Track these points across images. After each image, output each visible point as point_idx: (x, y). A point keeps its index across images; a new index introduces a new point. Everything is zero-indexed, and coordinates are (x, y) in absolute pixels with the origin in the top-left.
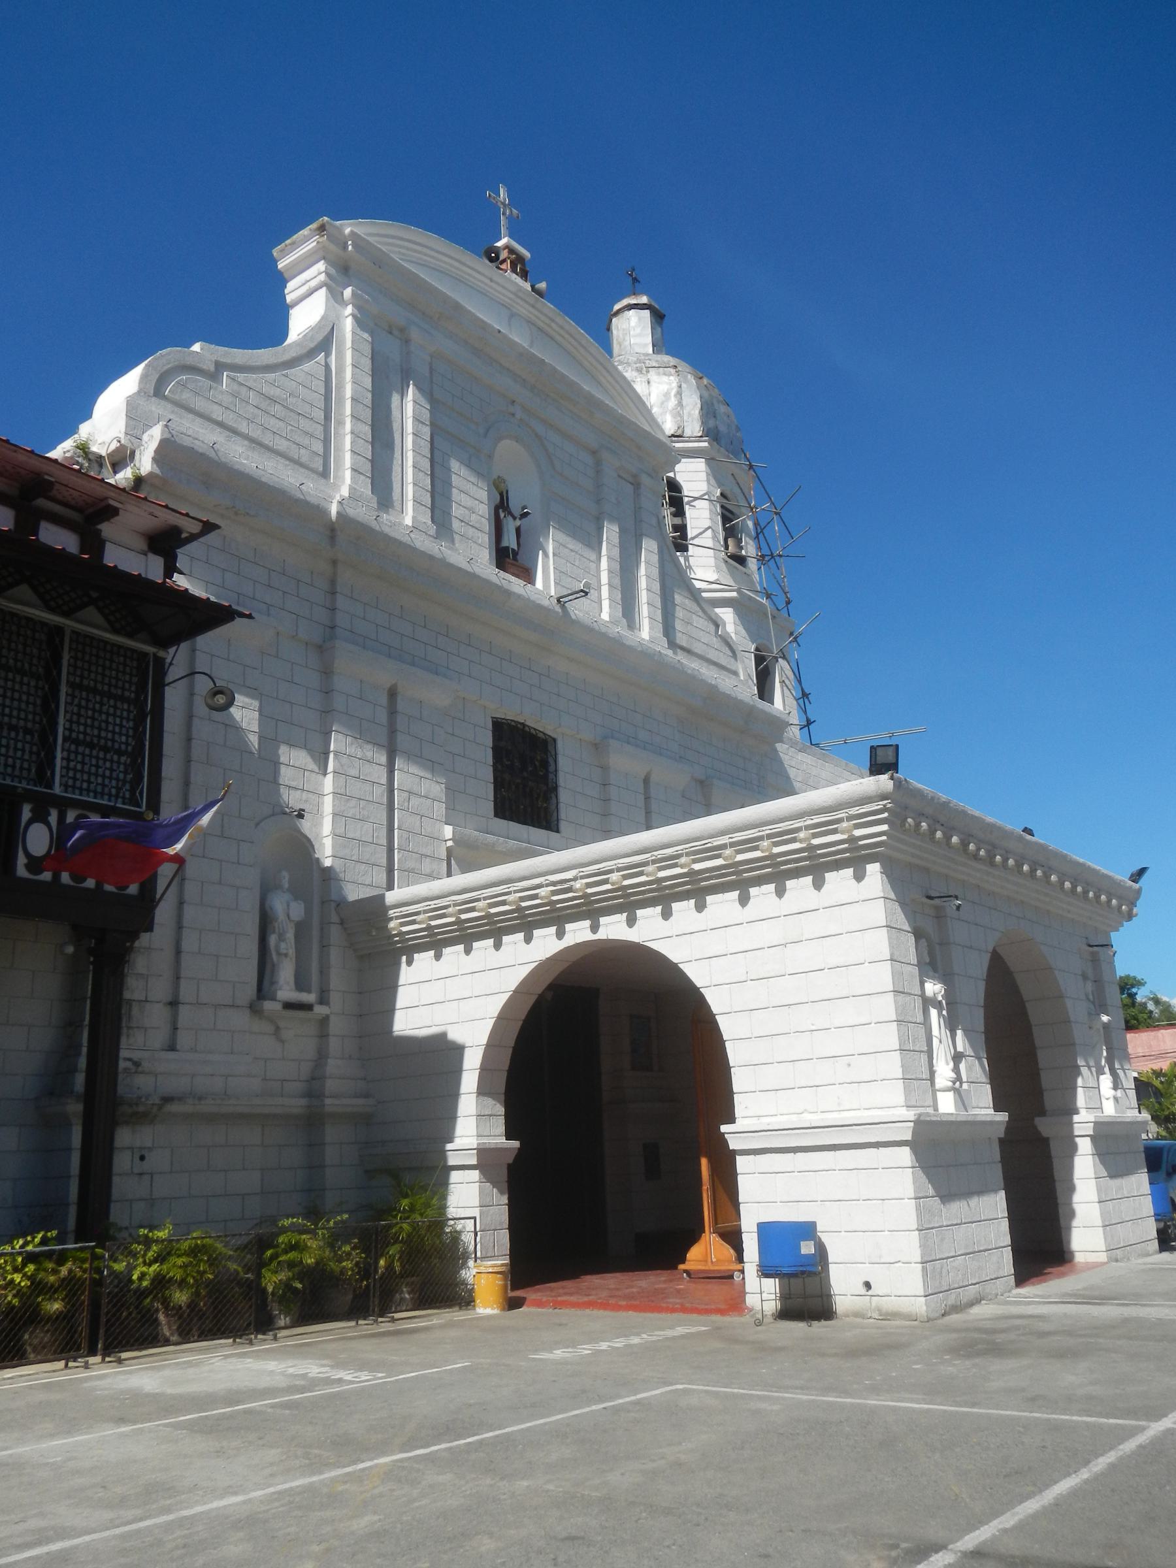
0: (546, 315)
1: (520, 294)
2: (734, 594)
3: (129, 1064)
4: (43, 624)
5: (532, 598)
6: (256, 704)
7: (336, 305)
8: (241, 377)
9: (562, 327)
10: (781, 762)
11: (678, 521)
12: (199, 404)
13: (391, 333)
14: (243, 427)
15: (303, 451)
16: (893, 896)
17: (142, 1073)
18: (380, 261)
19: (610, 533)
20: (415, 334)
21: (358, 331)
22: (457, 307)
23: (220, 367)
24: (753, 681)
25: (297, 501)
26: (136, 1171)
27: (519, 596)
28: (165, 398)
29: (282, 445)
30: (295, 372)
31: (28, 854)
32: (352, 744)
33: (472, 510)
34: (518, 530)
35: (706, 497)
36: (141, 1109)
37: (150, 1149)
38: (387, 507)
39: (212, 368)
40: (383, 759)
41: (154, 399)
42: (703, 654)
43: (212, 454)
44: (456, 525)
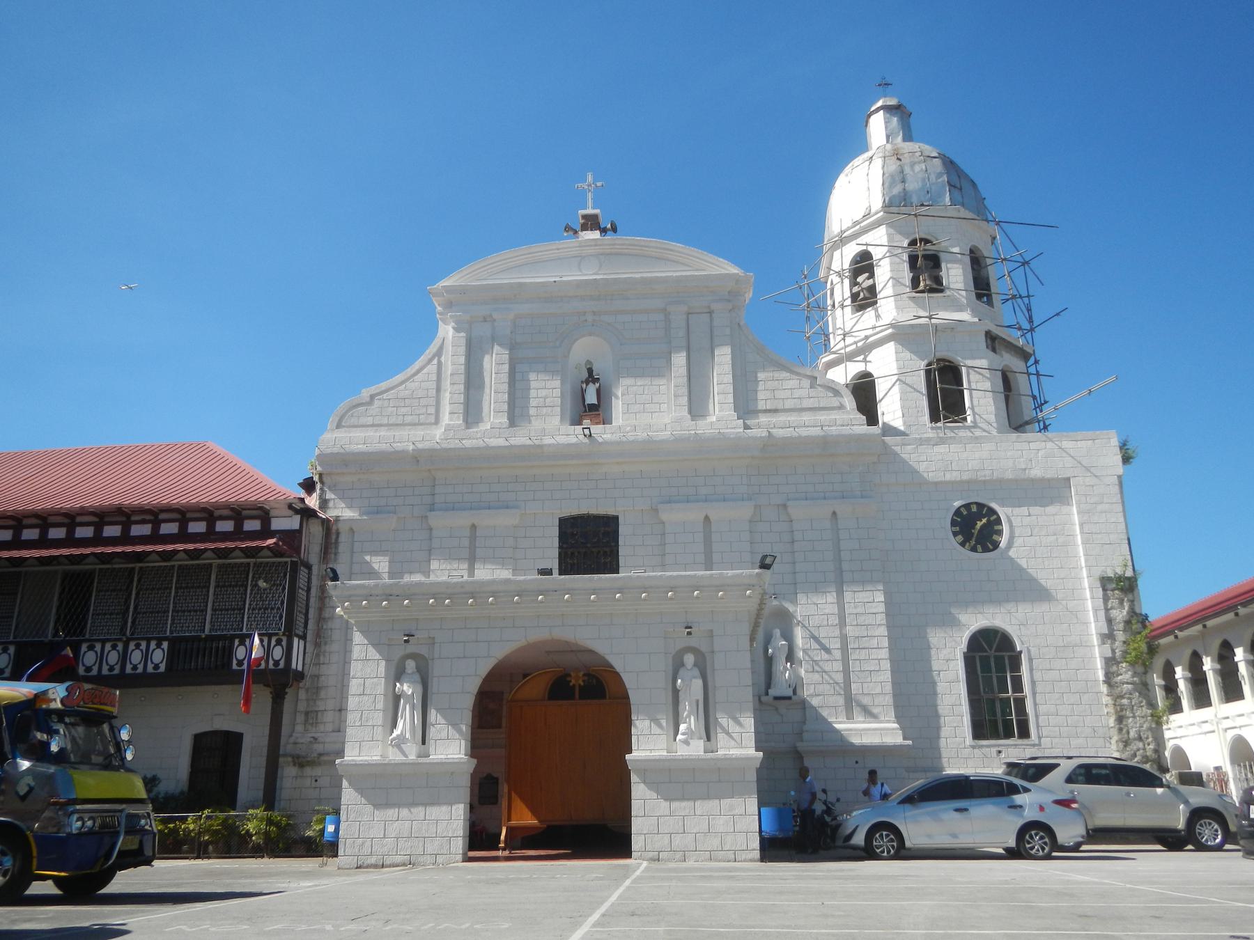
0: (607, 245)
1: (583, 244)
2: (890, 331)
3: (312, 739)
4: (242, 563)
5: (561, 443)
6: (387, 558)
7: (446, 326)
8: (385, 396)
9: (623, 245)
10: (904, 462)
11: (870, 282)
12: (363, 420)
13: (486, 321)
14: (385, 421)
15: (422, 417)
16: (366, 642)
17: (319, 743)
18: (463, 290)
19: (679, 360)
20: (495, 315)
21: (457, 334)
22: (521, 285)
23: (372, 397)
24: (921, 393)
25: (391, 453)
26: (313, 786)
27: (550, 445)
28: (344, 427)
29: (408, 419)
30: (419, 377)
31: (236, 659)
32: (444, 563)
33: (545, 398)
34: (598, 391)
35: (888, 255)
36: (309, 759)
37: (320, 777)
38: (477, 423)
39: (368, 399)
40: (466, 566)
41: (336, 430)
42: (792, 407)
43: (342, 451)
44: (532, 411)
